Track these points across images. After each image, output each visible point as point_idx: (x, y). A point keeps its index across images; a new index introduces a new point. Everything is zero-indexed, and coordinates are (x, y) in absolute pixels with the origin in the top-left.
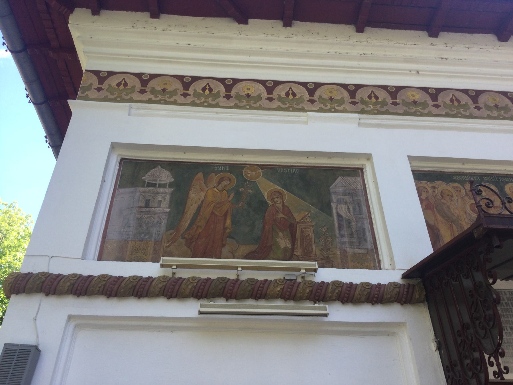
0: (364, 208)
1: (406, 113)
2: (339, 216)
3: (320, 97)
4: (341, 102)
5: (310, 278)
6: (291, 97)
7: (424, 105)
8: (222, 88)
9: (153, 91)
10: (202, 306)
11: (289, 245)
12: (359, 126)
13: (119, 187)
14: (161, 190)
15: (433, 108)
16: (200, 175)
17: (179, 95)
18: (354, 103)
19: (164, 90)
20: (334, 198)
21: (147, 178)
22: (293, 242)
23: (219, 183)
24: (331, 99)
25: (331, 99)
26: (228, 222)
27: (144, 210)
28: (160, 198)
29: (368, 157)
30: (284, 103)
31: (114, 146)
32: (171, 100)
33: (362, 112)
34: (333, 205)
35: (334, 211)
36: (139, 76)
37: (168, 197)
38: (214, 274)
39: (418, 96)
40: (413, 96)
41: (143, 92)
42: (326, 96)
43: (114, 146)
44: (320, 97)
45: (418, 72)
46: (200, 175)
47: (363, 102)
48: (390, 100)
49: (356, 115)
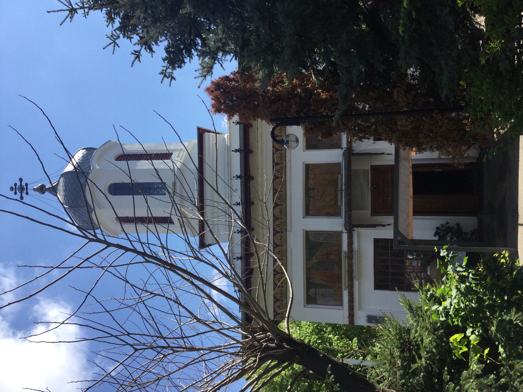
0: (321, 232)
1: (286, 216)
2: (323, 240)
3: (280, 243)
4: (282, 236)
5: (346, 253)
6: (280, 253)
7: (281, 209)
8: (278, 275)
9: (282, 297)
10: (356, 280)
11: (334, 255)
13: (317, 303)
14: (317, 291)
15: (283, 206)
16: (311, 280)
17: (283, 289)
18: (282, 232)
19: (281, 294)
20: (317, 241)
21: (313, 296)
22: (333, 254)
23: (314, 275)
24: (280, 239)
25: (280, 239)
26: (327, 272)
27: (324, 296)
28: (320, 292)
29: (303, 230)
30: (284, 255)
31: (304, 307)
32: (285, 291)
33: (286, 230)
34: (320, 241)
35: (322, 241)
36: (275, 302)
37: (320, 289)
38: (347, 277)
39: (278, 210)
40: (277, 212)
41: (282, 300)
42: (280, 241)
43: (304, 307)
44: (280, 243)
46: (311, 280)
47: (281, 229)
48: (280, 220)
49: (288, 232)
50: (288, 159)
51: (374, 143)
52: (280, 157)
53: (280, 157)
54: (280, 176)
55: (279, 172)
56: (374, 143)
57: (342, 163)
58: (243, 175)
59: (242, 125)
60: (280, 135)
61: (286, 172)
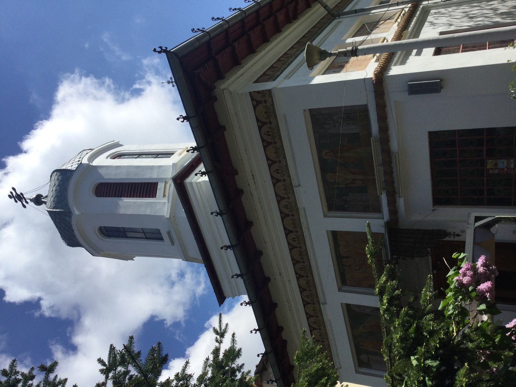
12: (326, 304)
45: (289, 281)
50: (304, 226)
51: (433, 210)
52: (292, 224)
53: (292, 224)
54: (298, 246)
55: (295, 241)
56: (433, 210)
57: (385, 234)
58: (244, 272)
59: (225, 216)
60: (286, 196)
61: (305, 242)
